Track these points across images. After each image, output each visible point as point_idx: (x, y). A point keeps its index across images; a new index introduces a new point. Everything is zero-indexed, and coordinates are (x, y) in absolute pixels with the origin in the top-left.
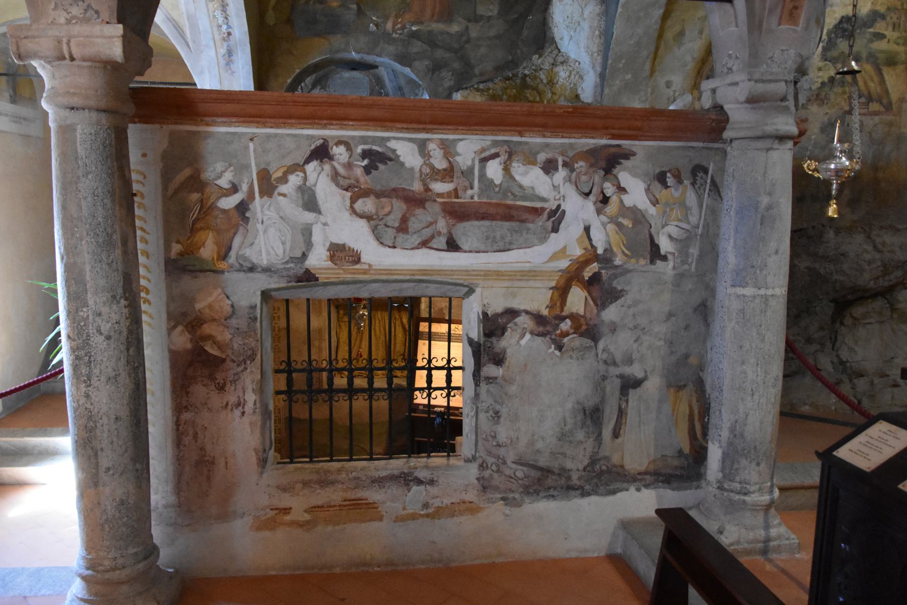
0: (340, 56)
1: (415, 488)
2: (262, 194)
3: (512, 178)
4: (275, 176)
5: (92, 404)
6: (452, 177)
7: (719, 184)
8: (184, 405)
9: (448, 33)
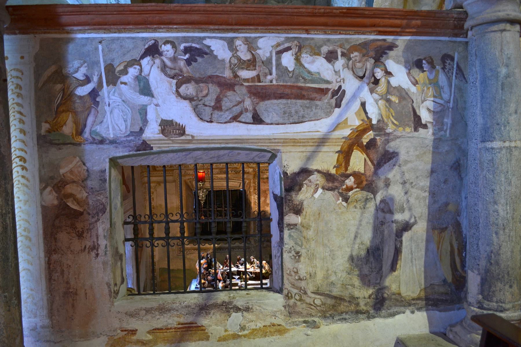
1: (234, 314)
2: (108, 84)
3: (302, 65)
4: (118, 69)
6: (255, 66)
7: (464, 70)
8: (53, 248)
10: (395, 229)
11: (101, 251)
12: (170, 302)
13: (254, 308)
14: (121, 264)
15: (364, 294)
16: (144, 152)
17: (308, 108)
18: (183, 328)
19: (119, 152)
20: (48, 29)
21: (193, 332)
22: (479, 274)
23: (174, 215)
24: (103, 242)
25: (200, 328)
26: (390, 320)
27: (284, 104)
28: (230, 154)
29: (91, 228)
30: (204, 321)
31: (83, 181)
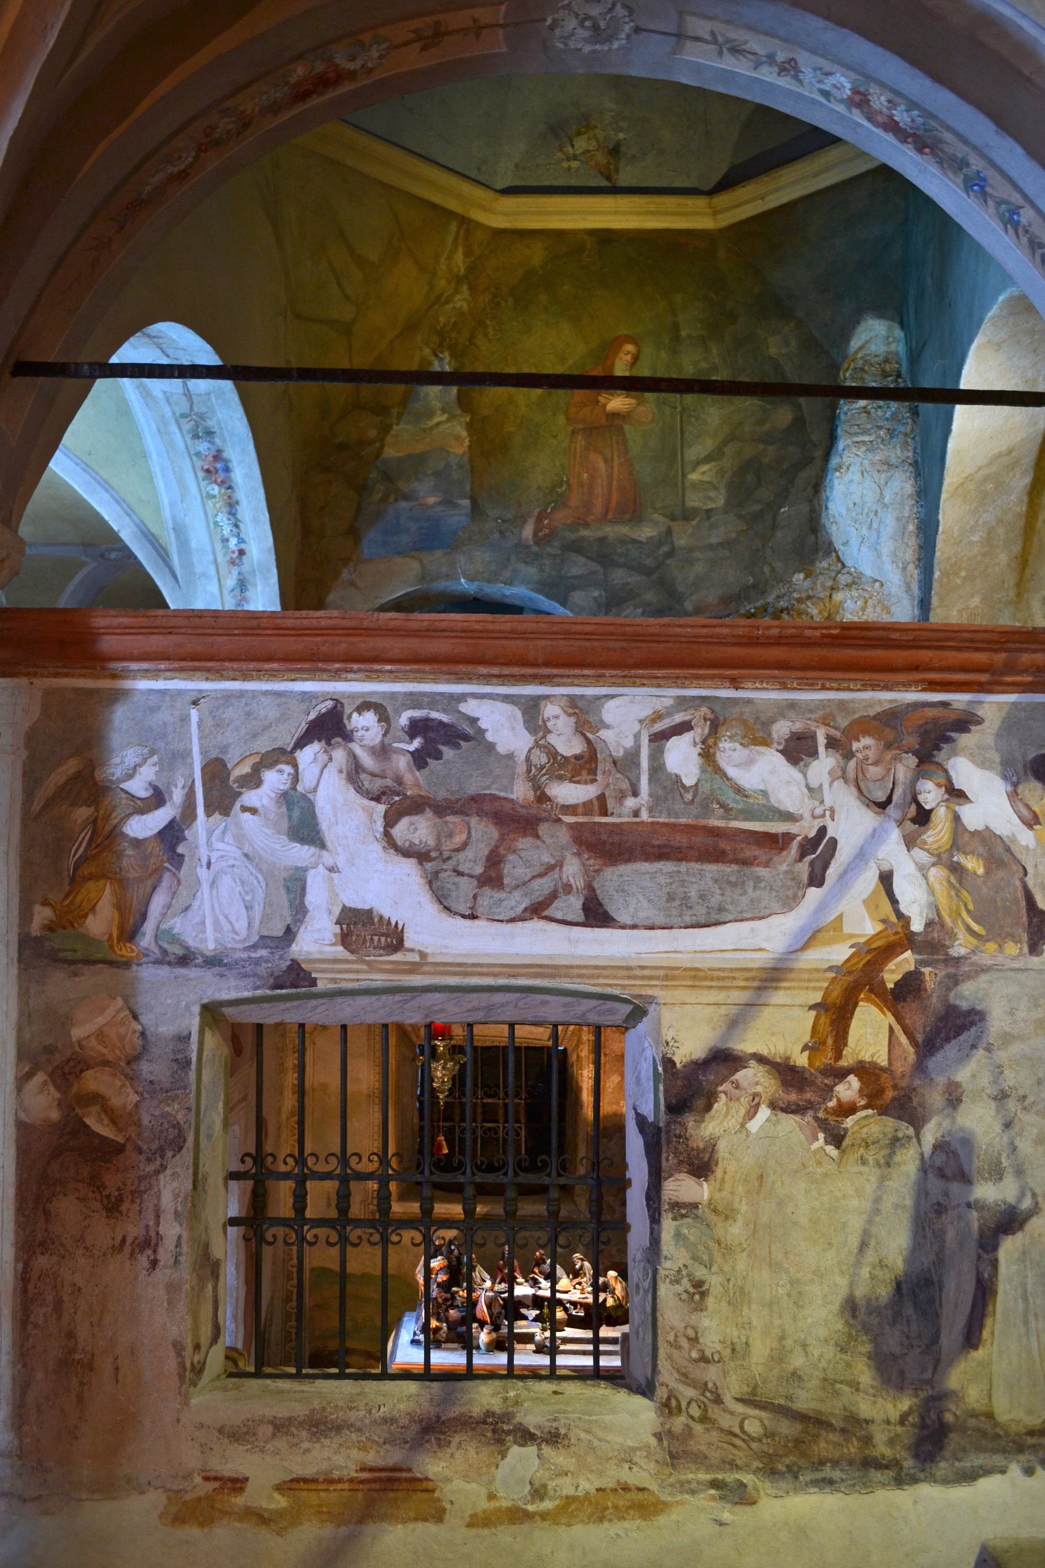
0: (441, 585)
1: (515, 1450)
3: (718, 770)
4: (237, 773)
6: (593, 772)
8: (39, 1237)
9: (635, 541)
10: (975, 1226)
11: (165, 1254)
12: (340, 1403)
13: (571, 1435)
14: (215, 1288)
15: (885, 1410)
16: (294, 991)
17: (734, 885)
18: (374, 1481)
19: (229, 988)
20: (64, 667)
21: (400, 1494)
23: (365, 1160)
24: (171, 1230)
25: (421, 1485)
26: (960, 1493)
27: (670, 875)
28: (521, 1004)
29: (142, 1188)
30: (433, 1466)
31: (129, 1063)
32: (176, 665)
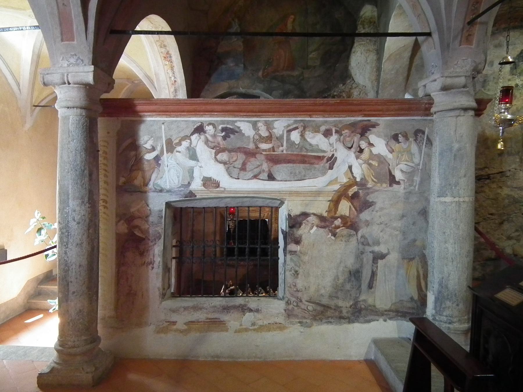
0: (234, 90)
3: (305, 140)
4: (175, 142)
5: (68, 257)
9: (293, 76)
17: (308, 170)
22: (434, 294)
32: (158, 113)
